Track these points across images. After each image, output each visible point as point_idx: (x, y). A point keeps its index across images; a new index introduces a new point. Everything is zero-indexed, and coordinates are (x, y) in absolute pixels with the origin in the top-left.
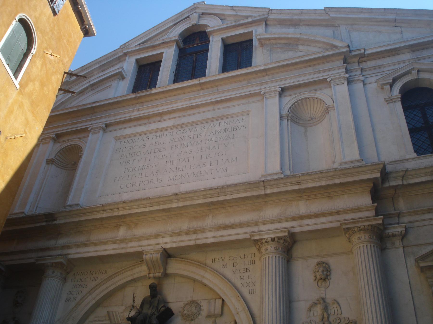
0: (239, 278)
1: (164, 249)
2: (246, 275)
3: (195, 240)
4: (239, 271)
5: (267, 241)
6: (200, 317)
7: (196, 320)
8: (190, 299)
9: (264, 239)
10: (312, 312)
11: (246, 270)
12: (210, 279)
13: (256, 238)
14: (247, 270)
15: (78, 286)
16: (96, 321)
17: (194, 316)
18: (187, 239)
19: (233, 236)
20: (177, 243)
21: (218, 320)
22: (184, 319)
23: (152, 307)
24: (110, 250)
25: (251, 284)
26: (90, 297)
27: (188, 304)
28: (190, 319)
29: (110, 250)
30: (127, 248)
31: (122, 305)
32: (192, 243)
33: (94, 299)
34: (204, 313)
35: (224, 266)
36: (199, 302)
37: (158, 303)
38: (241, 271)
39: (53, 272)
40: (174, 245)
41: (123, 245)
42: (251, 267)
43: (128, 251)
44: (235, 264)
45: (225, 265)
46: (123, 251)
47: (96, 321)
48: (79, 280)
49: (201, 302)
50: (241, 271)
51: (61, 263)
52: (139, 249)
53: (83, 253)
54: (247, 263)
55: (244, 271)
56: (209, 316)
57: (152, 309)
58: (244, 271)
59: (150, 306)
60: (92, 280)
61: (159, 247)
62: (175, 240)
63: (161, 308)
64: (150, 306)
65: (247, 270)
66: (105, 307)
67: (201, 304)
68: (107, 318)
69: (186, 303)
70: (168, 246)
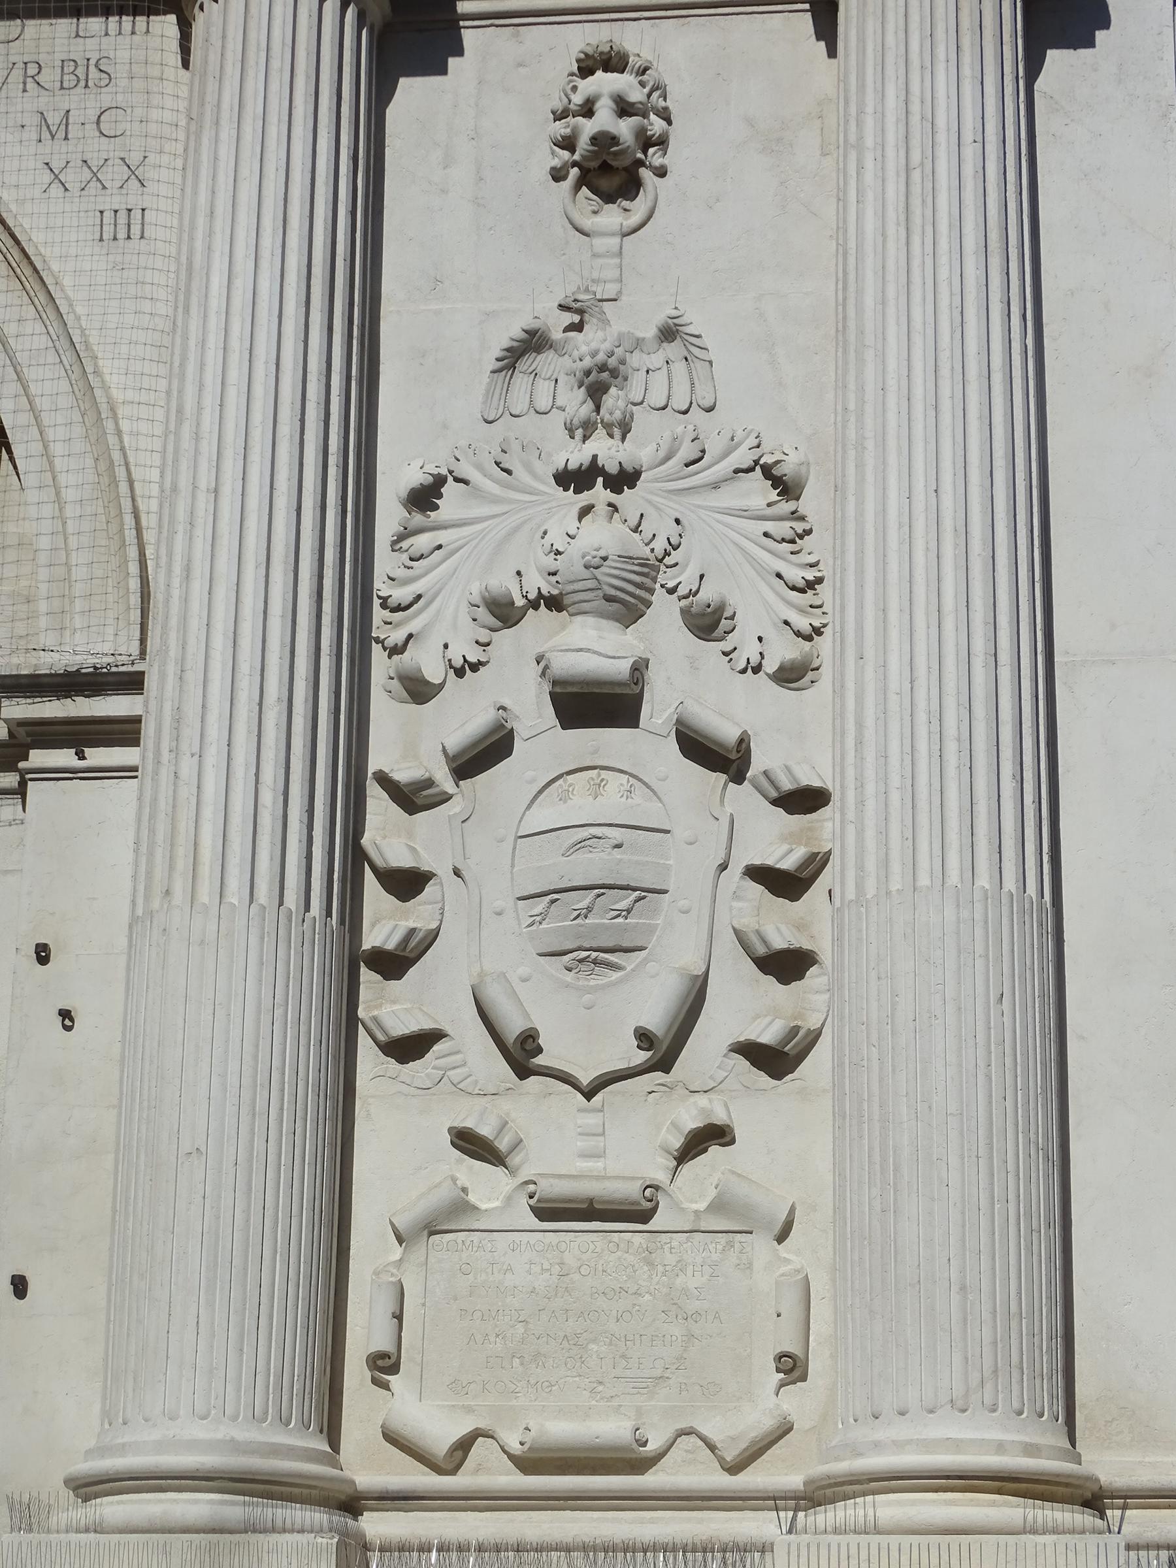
2: (82, 105)
10: (521, 382)
25: (114, 174)
38: (49, 77)
55: (69, 80)
58: (69, 80)
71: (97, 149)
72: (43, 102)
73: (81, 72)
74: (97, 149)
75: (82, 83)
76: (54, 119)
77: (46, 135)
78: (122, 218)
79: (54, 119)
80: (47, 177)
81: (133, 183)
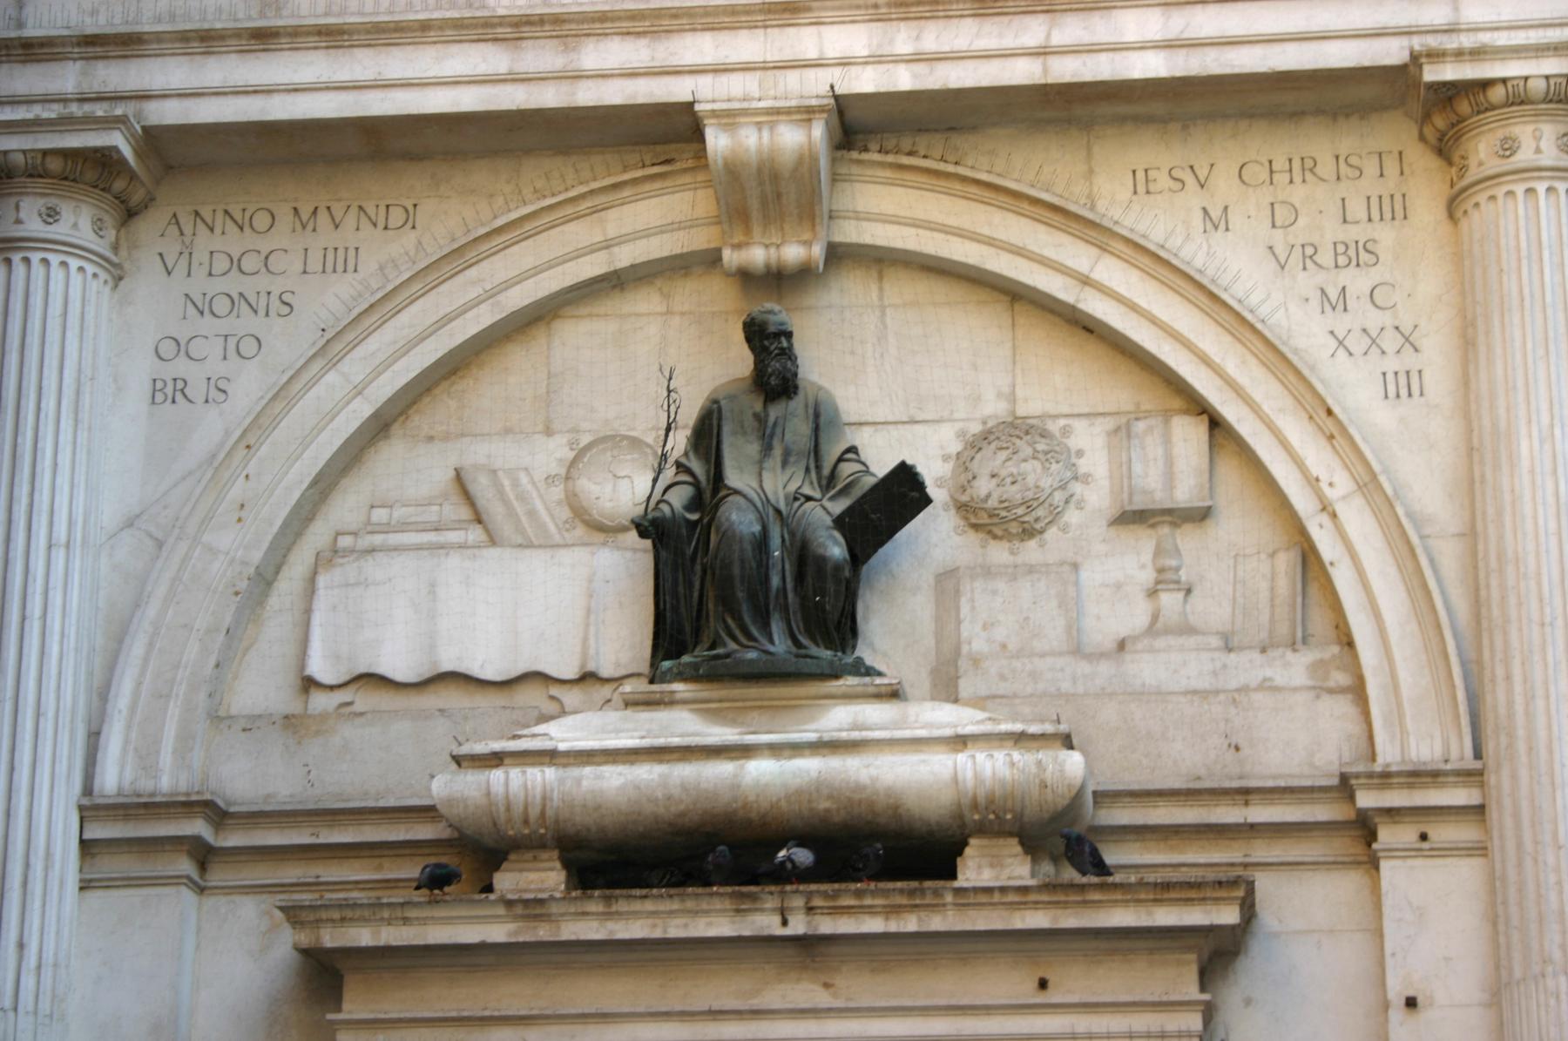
0: (1315, 297)
1: (836, 98)
2: (1358, 282)
3: (1043, 52)
4: (1309, 256)
5: (1518, 98)
6: (1072, 516)
7: (1052, 533)
8: (994, 408)
9: (1504, 81)
11: (1359, 254)
12: (1121, 295)
13: (1449, 72)
14: (1364, 256)
15: (222, 306)
16: (387, 529)
17: (1040, 512)
18: (983, 44)
19: (1291, 48)
20: (921, 68)
21: (1188, 540)
22: (976, 527)
23: (777, 452)
24: (456, 82)
25: (1390, 342)
26: (331, 377)
27: (986, 436)
28: (1014, 528)
29: (456, 82)
30: (578, 76)
31: (549, 432)
32: (1022, 73)
33: (359, 391)
34: (1098, 497)
35: (1216, 222)
36: (1054, 427)
37: (817, 429)
38: (1325, 257)
39: (51, 215)
40: (904, 80)
41: (540, 56)
42: (1385, 235)
43: (588, 95)
44: (1282, 214)
45: (1215, 213)
46: (550, 97)
47: (387, 529)
48: (221, 264)
49: (1066, 431)
50: (1325, 257)
51: (105, 160)
52: (676, 90)
53: (268, 91)
54: (1357, 209)
55: (1342, 260)
56: (1133, 517)
57: (785, 463)
58: (1342, 260)
59: (767, 449)
60: (315, 263)
61: (815, 86)
62: (903, 46)
63: (840, 460)
64: (767, 449)
65: (1364, 256)
66: (431, 439)
67: (1074, 443)
68: (465, 513)
69: (976, 428)
70: (865, 82)
71: (1374, 320)
72: (1320, 278)
73: (1352, 252)
74: (1374, 320)
75: (1354, 262)
76: (1333, 294)
77: (1327, 308)
78: (1403, 380)
79: (1333, 294)
80: (1333, 344)
81: (1408, 349)
